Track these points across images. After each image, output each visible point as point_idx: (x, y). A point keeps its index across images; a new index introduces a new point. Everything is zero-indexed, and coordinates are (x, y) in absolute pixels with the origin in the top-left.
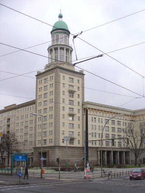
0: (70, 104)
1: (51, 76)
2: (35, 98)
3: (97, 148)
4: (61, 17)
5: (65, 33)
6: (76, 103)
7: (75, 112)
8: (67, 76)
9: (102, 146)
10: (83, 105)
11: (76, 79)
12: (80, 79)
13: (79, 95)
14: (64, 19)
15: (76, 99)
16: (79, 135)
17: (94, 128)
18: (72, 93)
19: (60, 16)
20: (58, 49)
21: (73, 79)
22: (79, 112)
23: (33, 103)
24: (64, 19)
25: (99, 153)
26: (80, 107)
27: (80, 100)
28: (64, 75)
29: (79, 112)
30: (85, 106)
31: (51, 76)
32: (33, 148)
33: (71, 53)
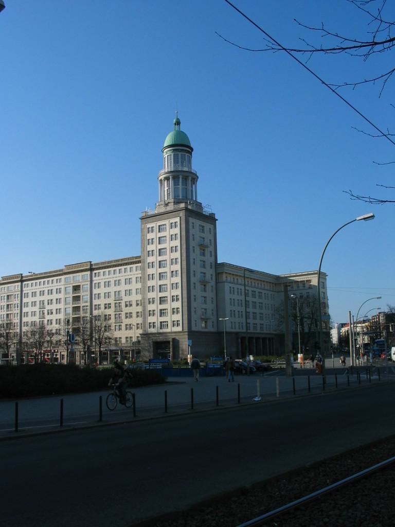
1: (173, 220)
2: (139, 254)
9: (248, 331)
10: (216, 268)
11: (208, 226)
13: (211, 252)
14: (183, 128)
17: (232, 303)
18: (203, 247)
19: (178, 123)
20: (179, 178)
21: (203, 227)
23: (136, 260)
24: (183, 128)
25: (240, 340)
26: (212, 271)
27: (212, 259)
32: (140, 334)
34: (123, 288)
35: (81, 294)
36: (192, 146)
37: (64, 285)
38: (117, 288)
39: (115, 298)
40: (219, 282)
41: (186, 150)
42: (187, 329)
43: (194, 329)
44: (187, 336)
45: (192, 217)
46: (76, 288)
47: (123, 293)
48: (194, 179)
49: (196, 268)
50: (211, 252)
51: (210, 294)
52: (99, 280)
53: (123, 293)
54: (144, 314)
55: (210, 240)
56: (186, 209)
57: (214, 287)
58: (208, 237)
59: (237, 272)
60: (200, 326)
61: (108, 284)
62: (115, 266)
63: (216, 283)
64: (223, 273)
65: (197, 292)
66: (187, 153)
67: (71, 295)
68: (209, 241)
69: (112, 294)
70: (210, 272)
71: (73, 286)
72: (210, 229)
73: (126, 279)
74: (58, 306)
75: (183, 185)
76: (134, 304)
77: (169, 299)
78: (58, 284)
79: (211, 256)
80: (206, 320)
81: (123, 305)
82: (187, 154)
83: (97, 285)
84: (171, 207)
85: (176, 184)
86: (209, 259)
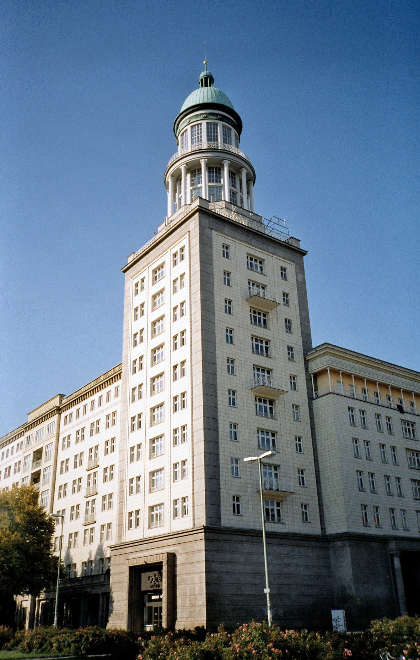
0: (257, 350)
3: (384, 540)
5: (223, 118)
6: (278, 350)
7: (280, 380)
8: (241, 249)
11: (273, 262)
13: (288, 321)
15: (274, 332)
16: (302, 482)
22: (294, 387)
25: (397, 563)
26: (298, 368)
27: (296, 340)
28: (228, 242)
29: (294, 387)
33: (248, 193)
36: (236, 110)
40: (318, 397)
41: (217, 115)
45: (216, 230)
55: (285, 295)
62: (93, 391)
63: (311, 399)
64: (324, 372)
65: (244, 415)
66: (220, 120)
82: (221, 123)
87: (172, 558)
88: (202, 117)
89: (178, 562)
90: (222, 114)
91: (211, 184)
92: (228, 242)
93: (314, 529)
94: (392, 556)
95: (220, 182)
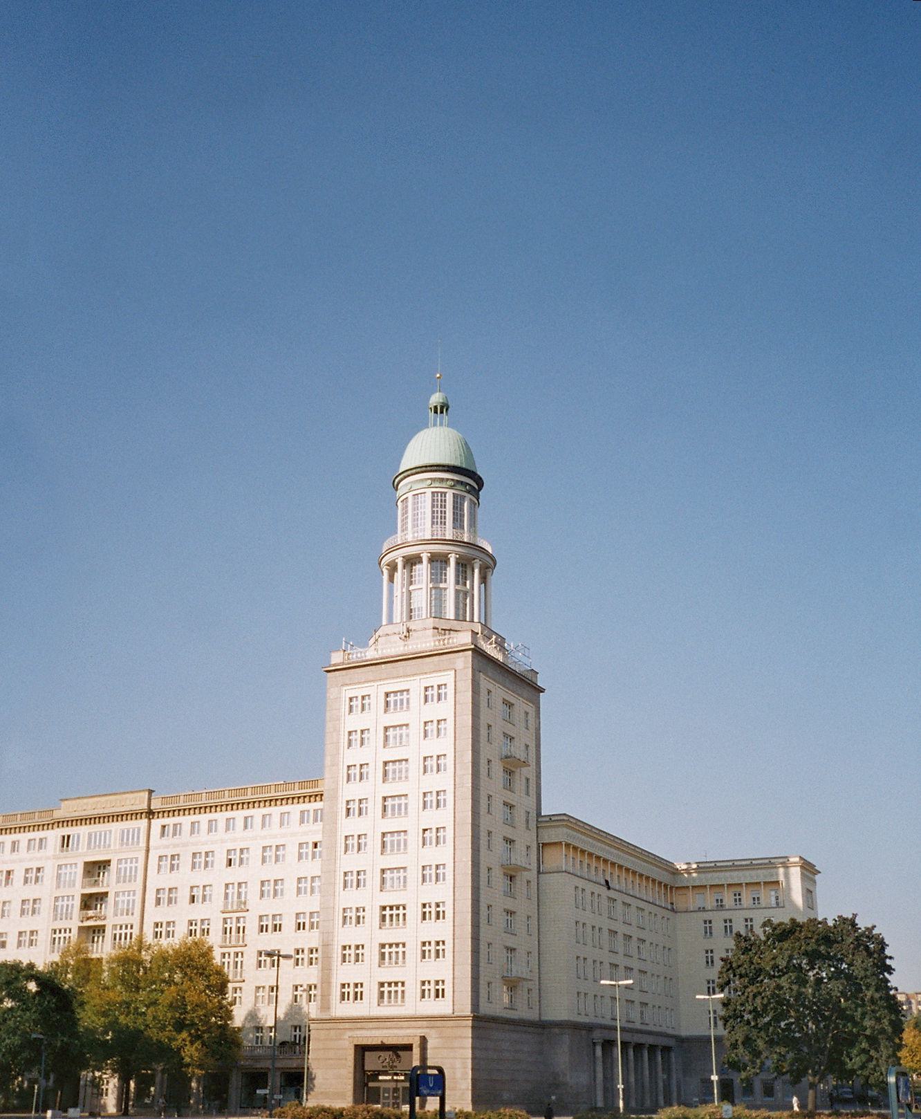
1: (434, 680)
4: (442, 408)
11: (521, 705)
12: (531, 709)
13: (528, 780)
18: (511, 766)
21: (510, 705)
30: (550, 835)
31: (434, 680)
34: (253, 872)
35: (109, 883)
37: (56, 857)
38: (235, 874)
39: (226, 905)
42: (469, 1007)
43: (485, 1009)
44: (469, 1032)
46: (95, 868)
47: (253, 891)
48: (488, 567)
49: (494, 820)
50: (528, 780)
51: (524, 907)
52: (175, 846)
53: (253, 891)
54: (327, 958)
55: (527, 746)
56: (478, 652)
57: (534, 885)
58: (524, 737)
59: (593, 846)
60: (499, 1003)
61: (202, 860)
62: (232, 806)
63: (539, 872)
65: (495, 894)
66: (469, 492)
67: (78, 888)
68: (523, 748)
69: (217, 893)
70: (525, 838)
71: (86, 864)
72: (527, 713)
73: (264, 848)
74: (27, 924)
75: (457, 582)
76: (289, 923)
77: (414, 913)
78: (35, 853)
79: (528, 794)
80: (512, 985)
81: (252, 925)
82: (469, 496)
83: (166, 864)
84: (425, 641)
85: (437, 577)
86: (524, 803)
87: (424, 1040)
88: (449, 483)
89: (429, 1045)
90: (467, 479)
91: (459, 587)
92: (491, 687)
93: (532, 1015)
94: (594, 1044)
95: (465, 584)
